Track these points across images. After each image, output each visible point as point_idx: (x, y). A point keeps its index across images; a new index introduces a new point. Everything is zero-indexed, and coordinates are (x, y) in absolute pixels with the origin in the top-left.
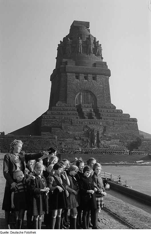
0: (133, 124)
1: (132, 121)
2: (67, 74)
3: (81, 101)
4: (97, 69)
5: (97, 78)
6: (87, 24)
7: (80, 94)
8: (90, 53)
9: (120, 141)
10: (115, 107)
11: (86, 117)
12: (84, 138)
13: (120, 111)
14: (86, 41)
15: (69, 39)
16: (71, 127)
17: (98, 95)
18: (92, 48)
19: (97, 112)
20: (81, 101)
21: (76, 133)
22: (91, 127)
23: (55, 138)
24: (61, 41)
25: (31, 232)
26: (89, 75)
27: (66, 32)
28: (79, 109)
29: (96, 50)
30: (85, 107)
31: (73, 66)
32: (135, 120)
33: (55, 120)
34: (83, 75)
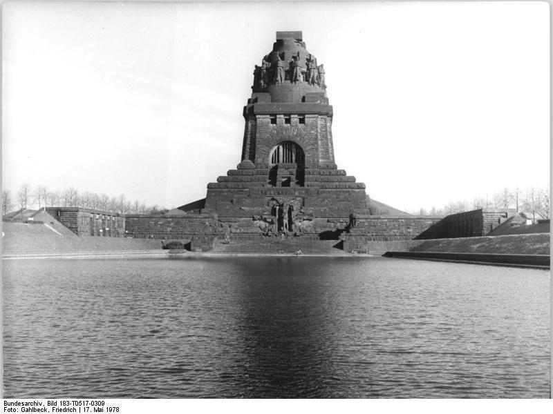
0: (359, 192)
1: (357, 189)
2: (257, 116)
5: (306, 119)
7: (278, 148)
8: (296, 80)
9: (328, 221)
10: (335, 167)
13: (342, 172)
14: (291, 63)
17: (308, 148)
18: (299, 72)
21: (256, 208)
22: (281, 199)
23: (213, 218)
24: (256, 66)
28: (273, 174)
29: (310, 75)
30: (284, 167)
34: (282, 116)
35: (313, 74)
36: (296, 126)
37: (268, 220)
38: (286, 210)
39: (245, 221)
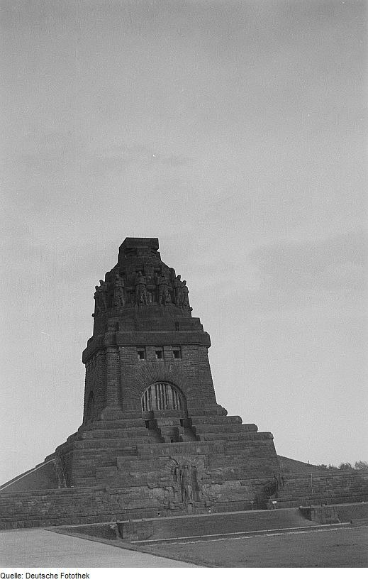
1: (263, 440)
3: (154, 404)
4: (181, 334)
6: (153, 243)
11: (167, 438)
12: (166, 484)
15: (118, 276)
16: (136, 463)
19: (188, 424)
20: (154, 404)
22: (181, 459)
23: (105, 491)
24: (101, 281)
25: (77, 575)
26: (165, 348)
27: (112, 261)
28: (151, 424)
31: (130, 332)
32: (268, 436)
33: (101, 451)
35: (175, 290)
36: (172, 361)
37: (167, 488)
38: (189, 474)
39: (138, 492)
